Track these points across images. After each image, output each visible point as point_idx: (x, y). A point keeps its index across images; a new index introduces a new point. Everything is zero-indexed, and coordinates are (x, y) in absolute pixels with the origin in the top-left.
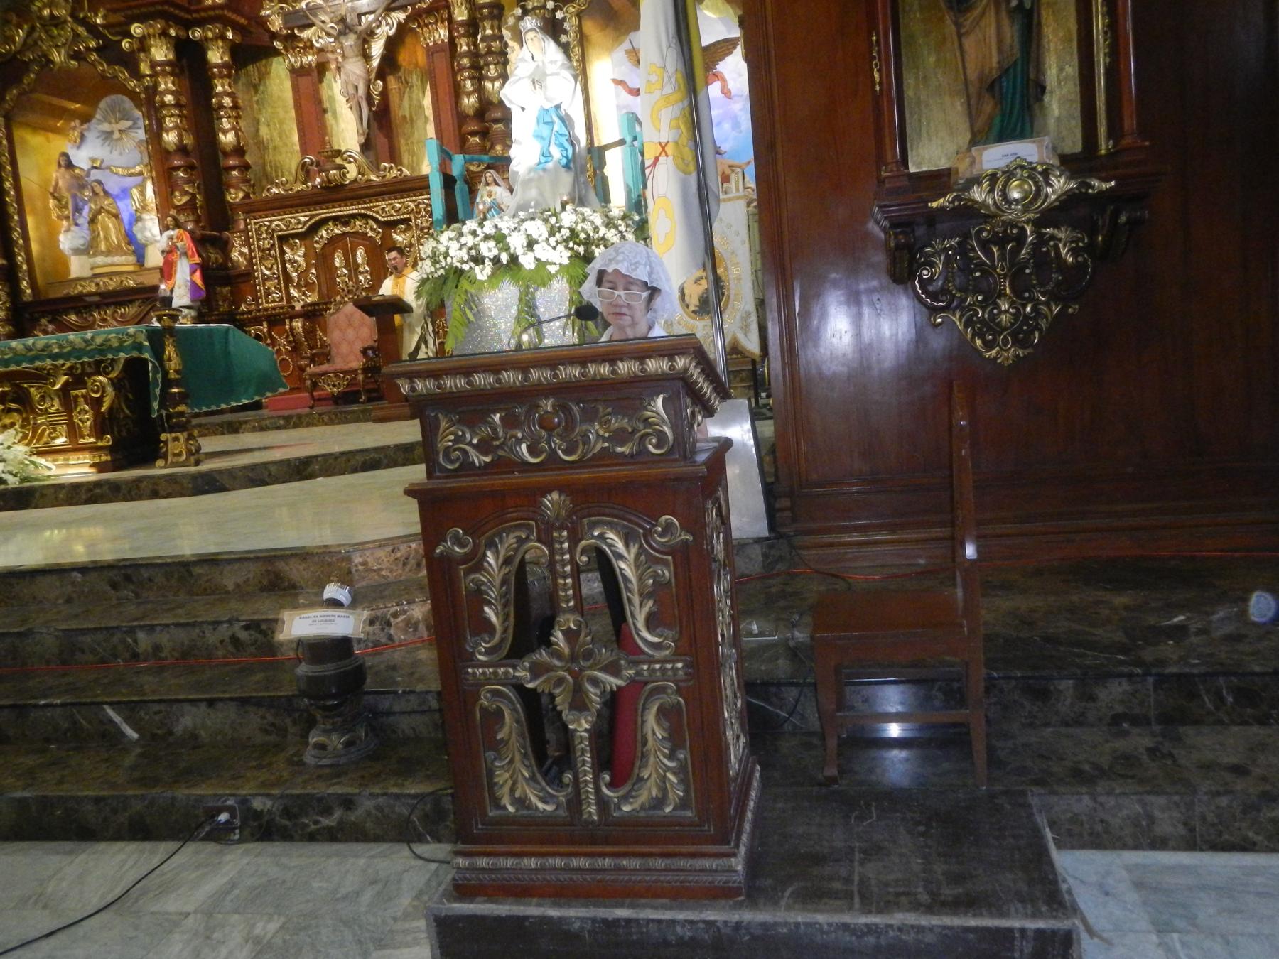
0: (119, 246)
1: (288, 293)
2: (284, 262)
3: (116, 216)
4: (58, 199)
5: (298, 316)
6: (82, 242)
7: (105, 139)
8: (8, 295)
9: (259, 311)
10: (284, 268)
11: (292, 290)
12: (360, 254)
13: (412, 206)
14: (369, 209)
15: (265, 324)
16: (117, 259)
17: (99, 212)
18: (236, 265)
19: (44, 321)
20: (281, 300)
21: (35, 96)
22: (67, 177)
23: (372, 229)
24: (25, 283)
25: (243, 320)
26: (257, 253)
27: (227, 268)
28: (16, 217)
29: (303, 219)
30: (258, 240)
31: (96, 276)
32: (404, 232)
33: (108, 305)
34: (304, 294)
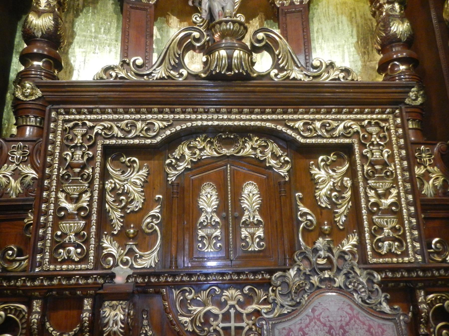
1: (99, 248)
2: (102, 191)
5: (119, 295)
9: (33, 278)
10: (102, 200)
11: (106, 243)
12: (251, 195)
13: (356, 127)
14: (282, 122)
15: (37, 306)
20: (84, 259)
23: (275, 156)
26: (56, 171)
29: (158, 124)
30: (64, 147)
32: (332, 165)
34: (131, 252)
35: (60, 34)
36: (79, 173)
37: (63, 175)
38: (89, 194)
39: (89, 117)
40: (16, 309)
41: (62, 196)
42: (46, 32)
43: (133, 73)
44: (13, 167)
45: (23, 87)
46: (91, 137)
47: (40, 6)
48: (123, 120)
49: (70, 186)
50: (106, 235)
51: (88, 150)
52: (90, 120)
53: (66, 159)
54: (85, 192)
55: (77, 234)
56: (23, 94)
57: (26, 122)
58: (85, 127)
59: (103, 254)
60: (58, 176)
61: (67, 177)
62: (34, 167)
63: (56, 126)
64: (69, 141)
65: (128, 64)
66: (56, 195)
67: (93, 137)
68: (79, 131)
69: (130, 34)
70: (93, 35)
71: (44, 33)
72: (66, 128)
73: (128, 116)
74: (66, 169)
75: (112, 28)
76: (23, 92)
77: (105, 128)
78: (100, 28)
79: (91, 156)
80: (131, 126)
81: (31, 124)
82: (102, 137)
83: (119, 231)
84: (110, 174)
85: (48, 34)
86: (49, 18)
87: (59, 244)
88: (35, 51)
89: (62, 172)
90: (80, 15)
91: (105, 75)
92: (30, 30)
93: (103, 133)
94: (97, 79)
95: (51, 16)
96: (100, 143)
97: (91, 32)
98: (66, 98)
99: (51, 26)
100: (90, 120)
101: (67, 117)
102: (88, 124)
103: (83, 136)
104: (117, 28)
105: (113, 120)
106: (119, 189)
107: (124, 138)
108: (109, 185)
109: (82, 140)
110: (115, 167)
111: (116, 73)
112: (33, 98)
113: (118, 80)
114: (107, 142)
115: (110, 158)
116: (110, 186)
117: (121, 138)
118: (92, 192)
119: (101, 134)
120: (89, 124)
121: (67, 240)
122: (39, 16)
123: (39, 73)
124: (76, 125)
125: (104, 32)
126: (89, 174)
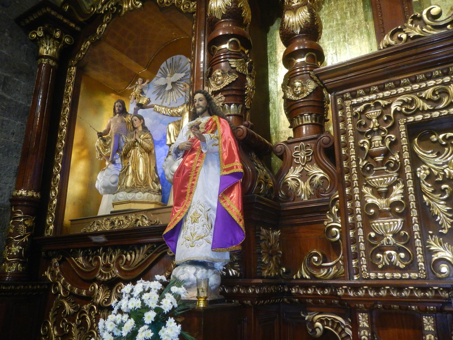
0: (146, 182)
2: (416, 180)
3: (149, 152)
4: (105, 140)
6: (114, 179)
7: (159, 94)
8: (29, 229)
16: (139, 196)
17: (134, 146)
18: (291, 195)
19: (55, 261)
21: (106, 48)
22: (118, 121)
24: (50, 219)
25: (302, 298)
26: (355, 163)
27: (277, 198)
28: (61, 153)
31: (114, 213)
33: (115, 248)
35: (317, 24)
36: (382, 162)
37: (364, 166)
38: (401, 186)
39: (381, 95)
40: (333, 321)
41: (367, 191)
42: (304, 26)
43: (429, 27)
44: (299, 169)
45: (293, 87)
46: (389, 117)
47: (293, 3)
48: (427, 88)
49: (375, 178)
50: (431, 235)
51: (388, 134)
52: (384, 98)
53: (363, 148)
54: (396, 183)
55: (396, 235)
56: (295, 94)
57: (302, 122)
58: (378, 107)
59: (434, 259)
60: (357, 168)
61: (368, 168)
62: (320, 166)
63: (344, 113)
64: (362, 127)
65: (421, 18)
66: (360, 189)
67: (392, 116)
68: (373, 113)
69: (382, 6)
70: (340, 22)
71: (303, 27)
72: (356, 113)
73: (431, 83)
74: (366, 159)
75: (359, 9)
76: (294, 92)
77: (404, 103)
78: (346, 13)
79: (393, 140)
80: (440, 93)
81: (307, 122)
82: (403, 115)
83: (449, 229)
84: (420, 159)
85: (307, 27)
86: (304, 11)
87: (375, 246)
88: (296, 48)
89: (362, 163)
90: (322, 7)
91: (393, 40)
92: (289, 30)
93: (404, 109)
94: (384, 48)
95: (305, 9)
96: (402, 122)
97: (337, 20)
98: (350, 79)
99: (307, 18)
100: (384, 98)
101: (355, 101)
102: (382, 103)
103: (378, 118)
104: (364, 7)
105: (413, 92)
106: (437, 176)
107: (434, 110)
108: (423, 172)
109: (378, 123)
110: (425, 148)
111: (407, 33)
112: (305, 95)
113: (410, 42)
114: (411, 119)
115: (416, 139)
116: (424, 173)
117: (429, 111)
118: (405, 183)
119: (401, 112)
120: (384, 103)
121: (384, 241)
122: (295, 13)
123: (304, 69)
124: (367, 108)
125: (351, 15)
126: (396, 161)
